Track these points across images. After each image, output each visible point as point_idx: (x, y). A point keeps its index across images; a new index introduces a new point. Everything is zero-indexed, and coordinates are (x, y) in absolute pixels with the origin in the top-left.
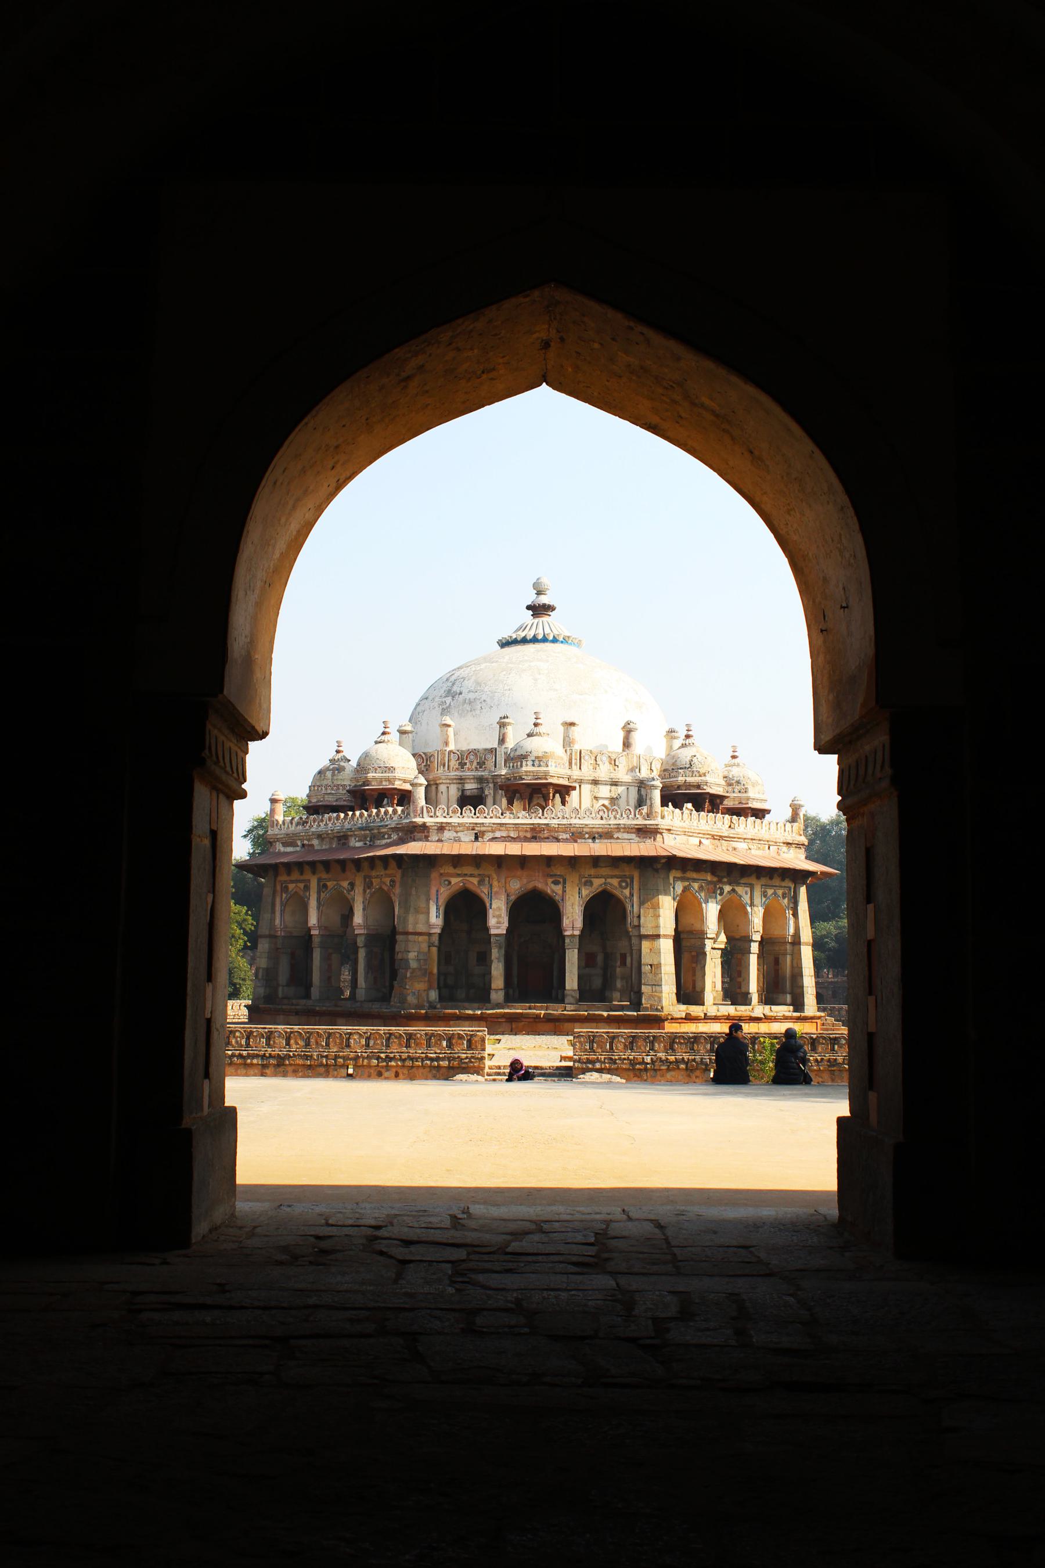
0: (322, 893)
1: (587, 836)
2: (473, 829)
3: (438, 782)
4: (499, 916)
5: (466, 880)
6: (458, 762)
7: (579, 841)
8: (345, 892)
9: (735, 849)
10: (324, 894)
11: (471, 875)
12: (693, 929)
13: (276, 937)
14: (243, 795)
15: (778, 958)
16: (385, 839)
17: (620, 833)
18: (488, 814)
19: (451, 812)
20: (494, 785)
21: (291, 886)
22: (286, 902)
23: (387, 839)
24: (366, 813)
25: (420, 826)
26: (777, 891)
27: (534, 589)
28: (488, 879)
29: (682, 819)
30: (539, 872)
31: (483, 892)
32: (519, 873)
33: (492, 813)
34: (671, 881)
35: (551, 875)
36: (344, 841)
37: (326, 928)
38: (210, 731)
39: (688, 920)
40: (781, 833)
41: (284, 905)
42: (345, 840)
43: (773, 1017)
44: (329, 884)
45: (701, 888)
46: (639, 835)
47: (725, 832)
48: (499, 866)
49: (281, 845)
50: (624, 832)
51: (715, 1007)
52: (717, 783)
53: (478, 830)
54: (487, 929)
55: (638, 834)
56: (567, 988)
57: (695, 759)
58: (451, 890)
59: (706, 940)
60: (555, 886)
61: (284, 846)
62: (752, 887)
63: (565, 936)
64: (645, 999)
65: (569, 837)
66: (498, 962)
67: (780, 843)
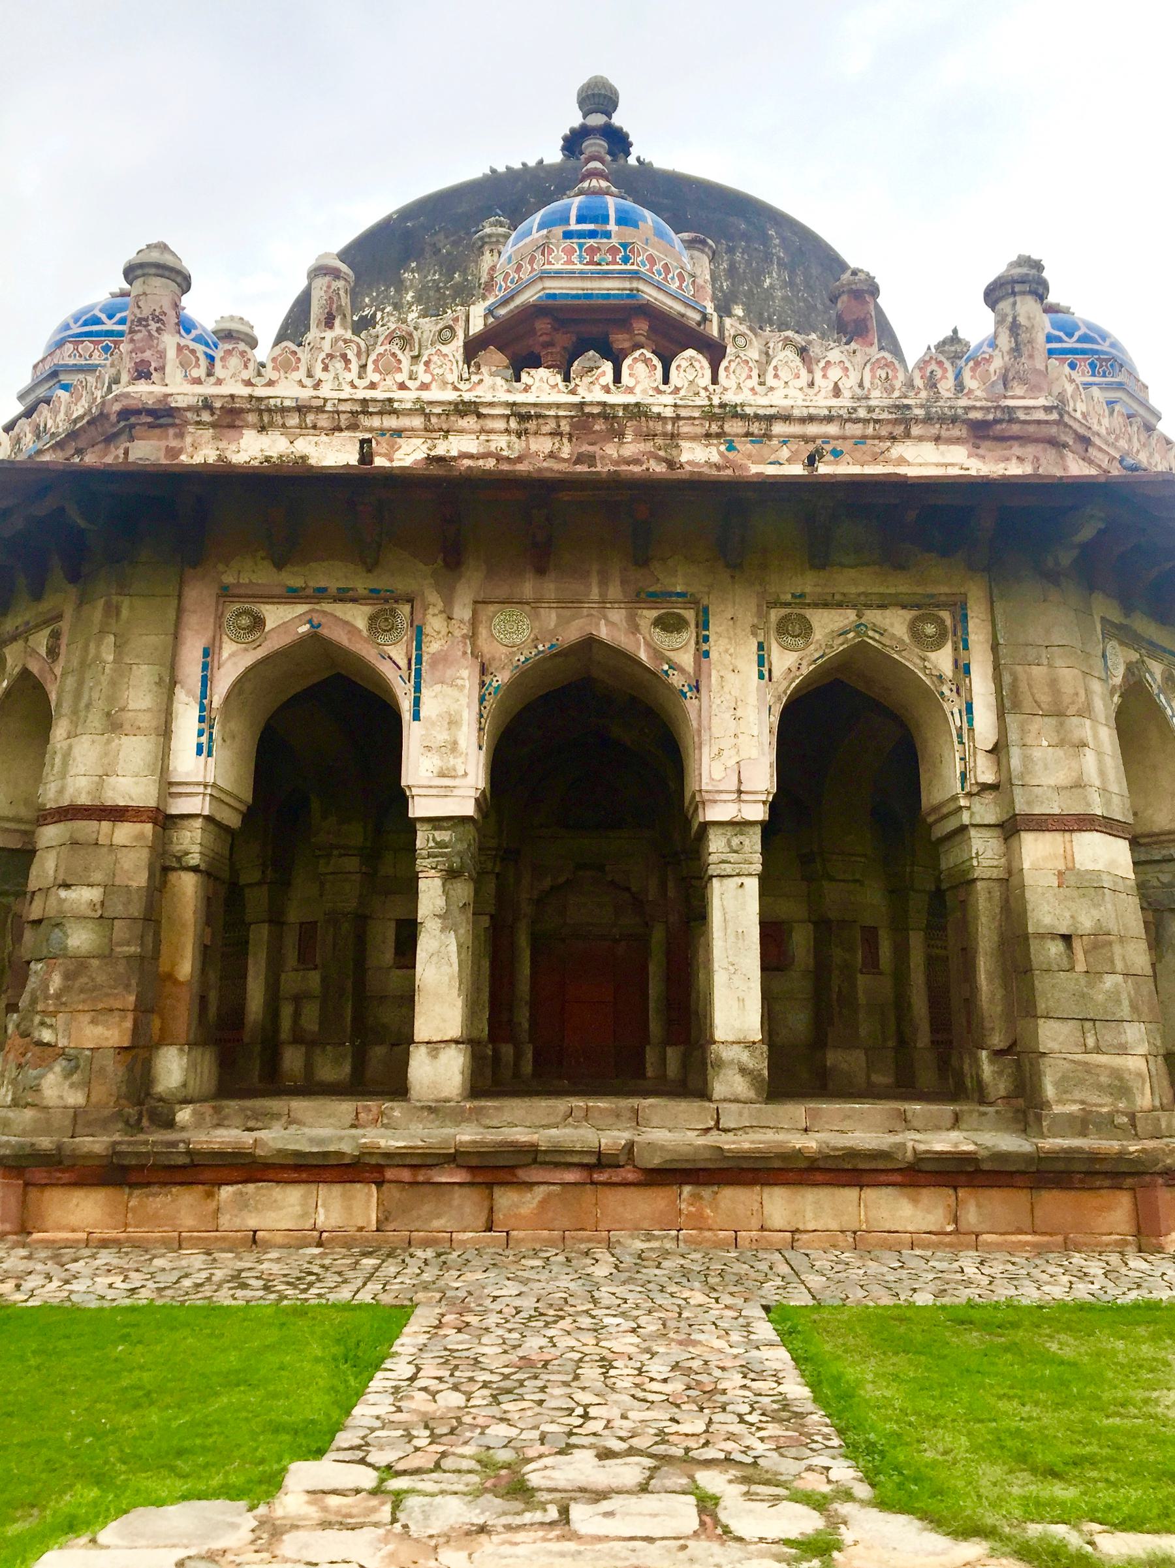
1: (785, 453)
2: (353, 427)
4: (454, 747)
11: (344, 596)
17: (909, 443)
25: (151, 412)
28: (406, 609)
30: (604, 583)
32: (528, 588)
46: (980, 451)
50: (921, 439)
53: (371, 430)
54: (401, 799)
55: (978, 448)
56: (720, 1034)
58: (260, 653)
63: (705, 826)
64: (1056, 1084)
66: (442, 930)
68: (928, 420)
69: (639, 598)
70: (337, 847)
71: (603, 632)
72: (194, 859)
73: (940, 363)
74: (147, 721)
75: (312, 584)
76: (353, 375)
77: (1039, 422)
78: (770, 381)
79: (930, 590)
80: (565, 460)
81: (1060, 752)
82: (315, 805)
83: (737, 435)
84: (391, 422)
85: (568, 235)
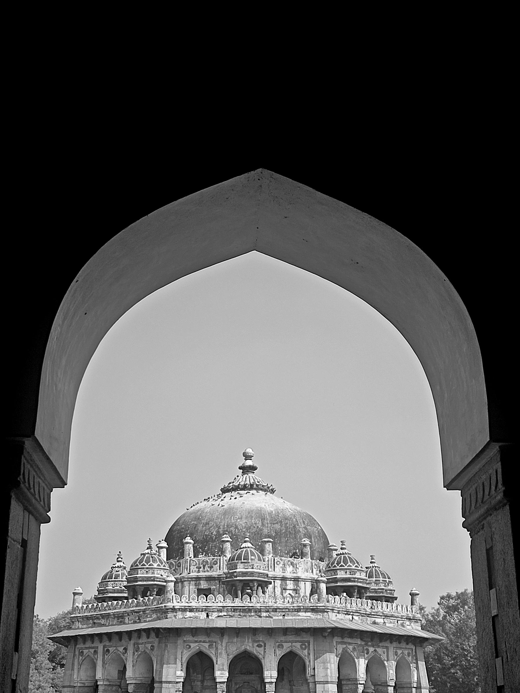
0: (106, 656)
2: (205, 611)
3: (183, 580)
5: (201, 645)
6: (196, 566)
7: (274, 618)
8: (121, 654)
9: (374, 623)
10: (107, 656)
11: (204, 642)
12: (350, 678)
13: (75, 686)
14: (48, 520)
16: (148, 618)
19: (191, 599)
20: (219, 582)
21: (85, 651)
22: (82, 663)
23: (149, 618)
24: (135, 601)
27: (244, 456)
28: (215, 644)
30: (248, 639)
31: (212, 653)
33: (218, 599)
35: (256, 641)
36: (121, 620)
37: (107, 679)
38: (24, 464)
39: (346, 671)
40: (405, 612)
41: (80, 665)
42: (122, 619)
44: (110, 649)
45: (354, 649)
47: (369, 611)
48: (223, 635)
49: (79, 623)
50: (302, 612)
54: (215, 679)
58: (191, 652)
59: (359, 685)
60: (258, 648)
61: (81, 624)
62: (387, 648)
69: (254, 641)
70: (196, 680)
71: (248, 648)
75: (199, 640)
76: (205, 601)
79: (304, 639)
81: (324, 670)
82: (191, 671)
85: (242, 563)
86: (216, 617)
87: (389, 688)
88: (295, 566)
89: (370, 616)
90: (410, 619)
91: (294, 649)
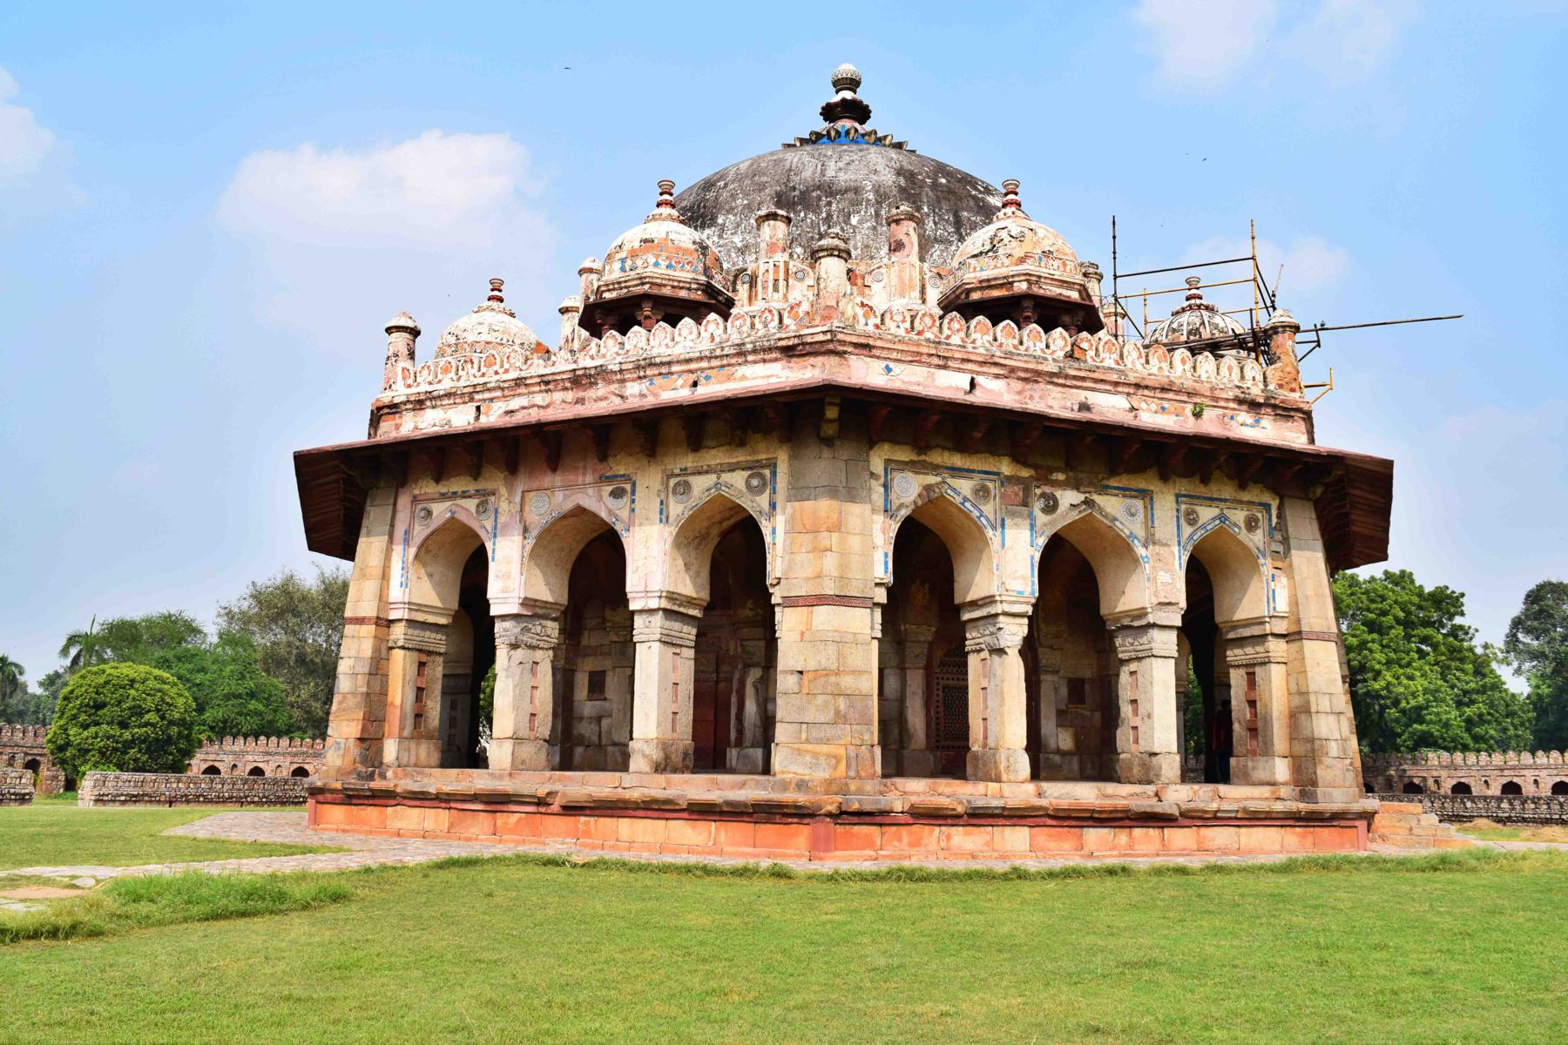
1: (680, 382)
2: (472, 400)
11: (465, 495)
15: (1254, 673)
18: (502, 366)
25: (389, 407)
26: (1225, 511)
29: (912, 328)
30: (584, 474)
31: (483, 527)
32: (548, 479)
34: (877, 463)
35: (608, 477)
43: (1206, 812)
45: (982, 492)
46: (791, 365)
50: (755, 362)
51: (1031, 788)
52: (1055, 277)
53: (480, 400)
54: (488, 605)
57: (1003, 234)
58: (429, 531)
59: (1001, 618)
62: (1144, 494)
65: (645, 391)
66: (507, 677)
67: (1227, 400)
68: (754, 351)
72: (400, 643)
73: (770, 311)
74: (378, 572)
76: (475, 371)
77: (821, 342)
78: (676, 339)
80: (570, 403)
83: (655, 375)
84: (487, 395)
86: (499, 416)
87: (1155, 634)
88: (859, 281)
89: (1061, 381)
90: (1253, 406)
91: (725, 491)
